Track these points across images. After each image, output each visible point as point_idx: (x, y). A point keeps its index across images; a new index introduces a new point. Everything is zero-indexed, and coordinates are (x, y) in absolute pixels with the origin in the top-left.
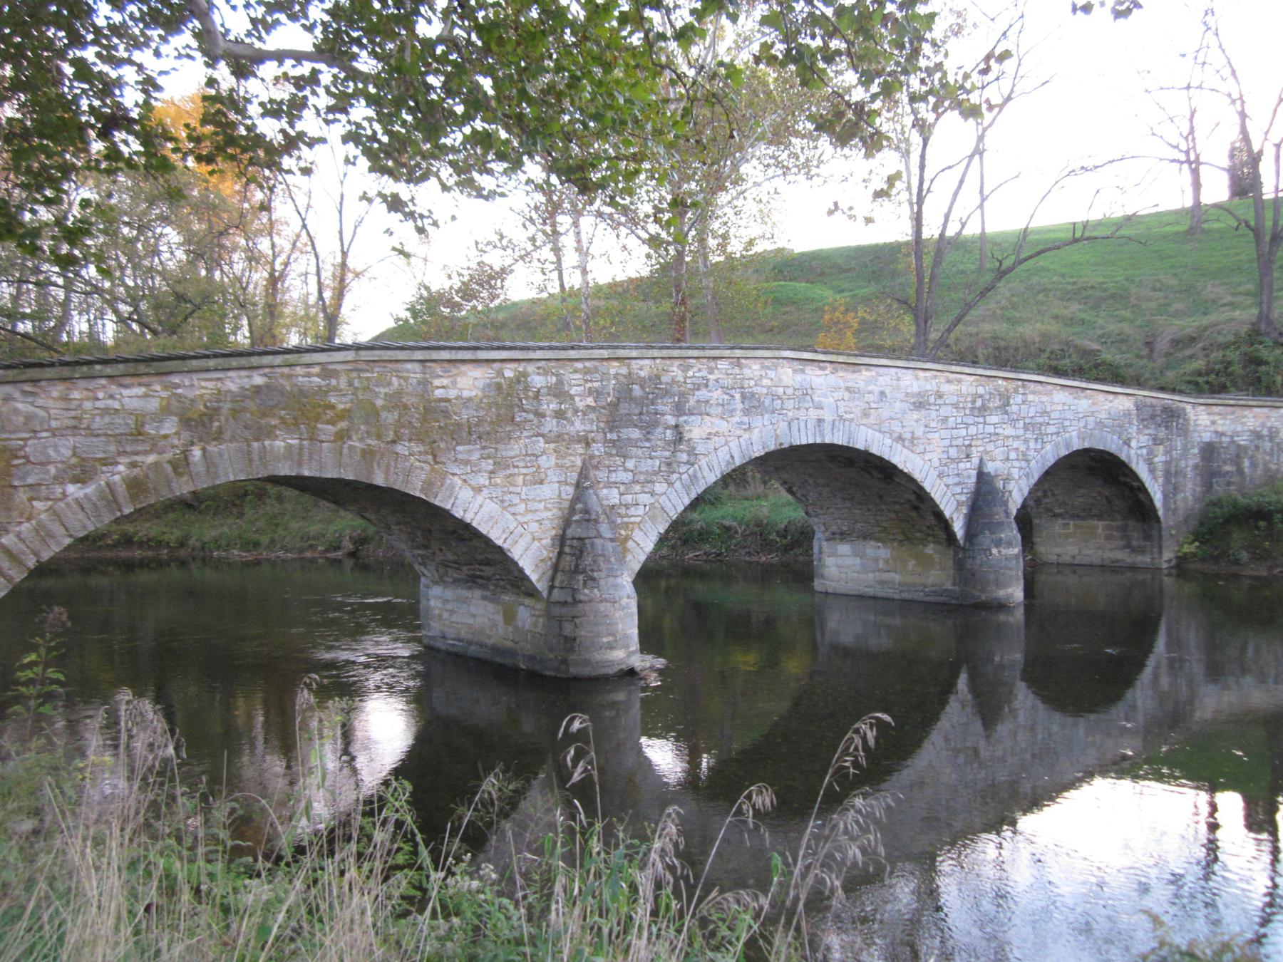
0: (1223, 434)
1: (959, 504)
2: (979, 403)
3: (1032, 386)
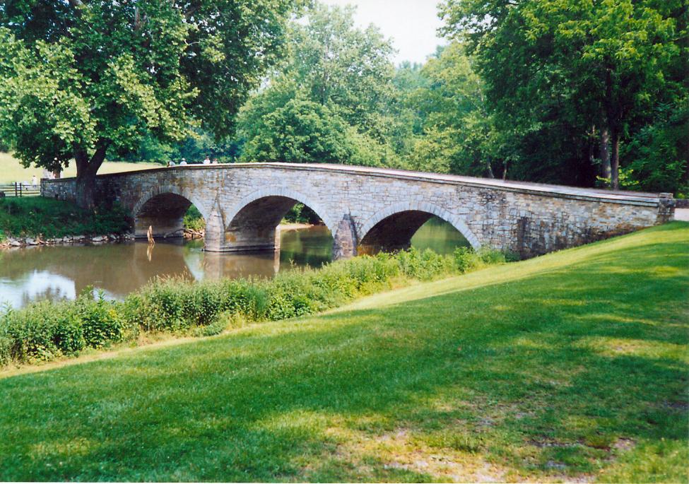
0: (532, 213)
1: (335, 225)
2: (345, 185)
3: (378, 178)
